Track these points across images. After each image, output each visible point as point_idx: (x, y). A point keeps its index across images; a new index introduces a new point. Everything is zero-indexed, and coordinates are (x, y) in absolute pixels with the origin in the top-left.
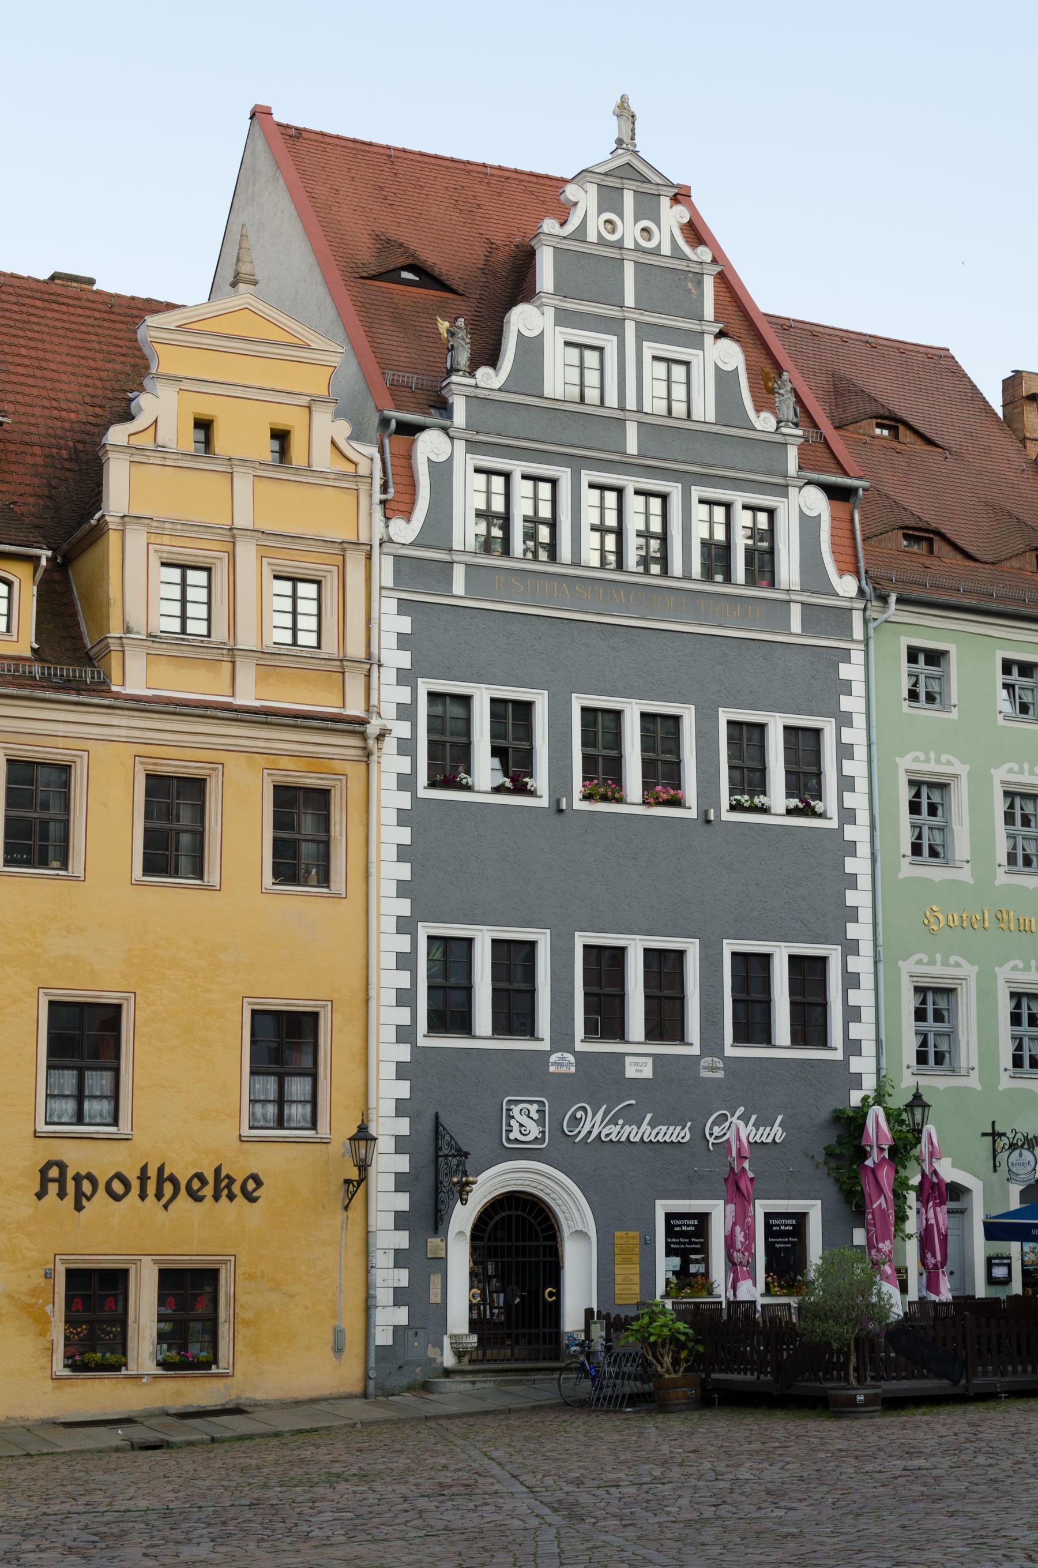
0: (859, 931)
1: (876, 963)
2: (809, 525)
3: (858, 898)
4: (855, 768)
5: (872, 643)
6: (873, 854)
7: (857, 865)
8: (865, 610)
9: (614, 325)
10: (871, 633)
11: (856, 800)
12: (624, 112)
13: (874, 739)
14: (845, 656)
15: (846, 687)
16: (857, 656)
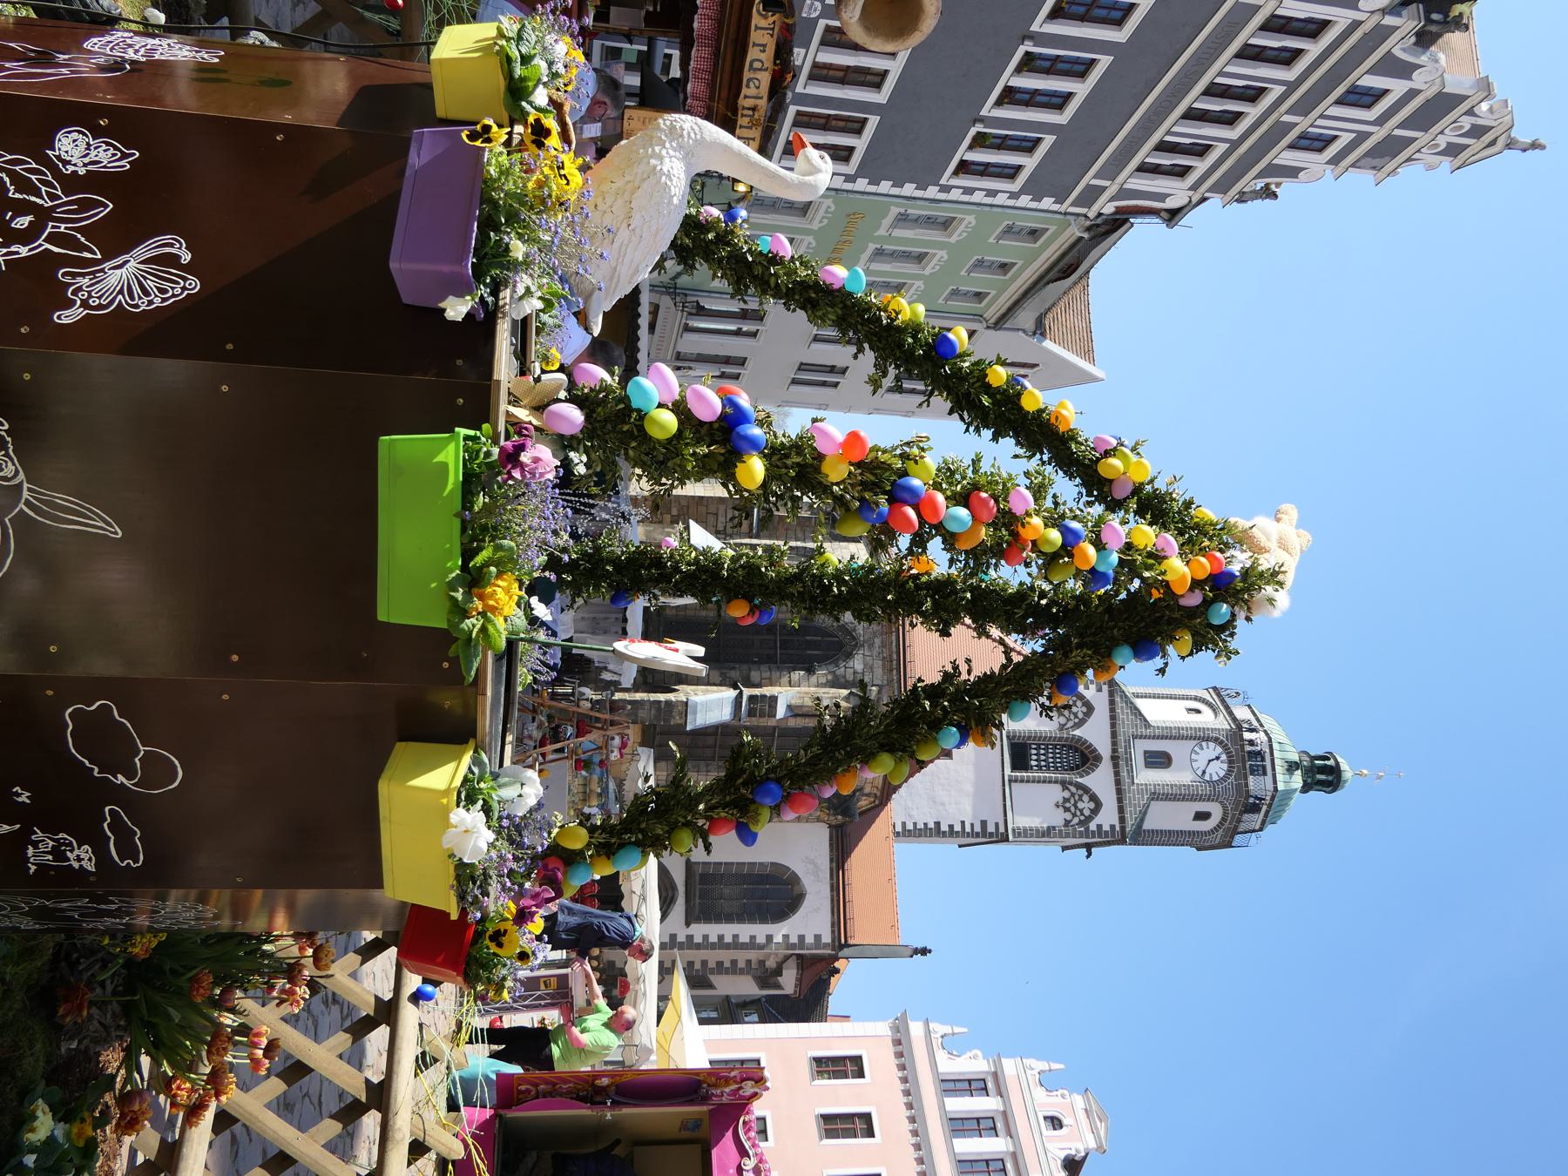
0: (862, 184)
1: (836, 190)
2: (1162, 197)
3: (885, 186)
4: (978, 197)
5: (1062, 217)
6: (914, 198)
7: (909, 189)
8: (1086, 216)
9: (1381, 121)
10: (1068, 217)
11: (955, 195)
12: (1535, 145)
13: (995, 209)
14: (1060, 201)
15: (1038, 199)
16: (1056, 207)
